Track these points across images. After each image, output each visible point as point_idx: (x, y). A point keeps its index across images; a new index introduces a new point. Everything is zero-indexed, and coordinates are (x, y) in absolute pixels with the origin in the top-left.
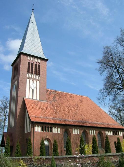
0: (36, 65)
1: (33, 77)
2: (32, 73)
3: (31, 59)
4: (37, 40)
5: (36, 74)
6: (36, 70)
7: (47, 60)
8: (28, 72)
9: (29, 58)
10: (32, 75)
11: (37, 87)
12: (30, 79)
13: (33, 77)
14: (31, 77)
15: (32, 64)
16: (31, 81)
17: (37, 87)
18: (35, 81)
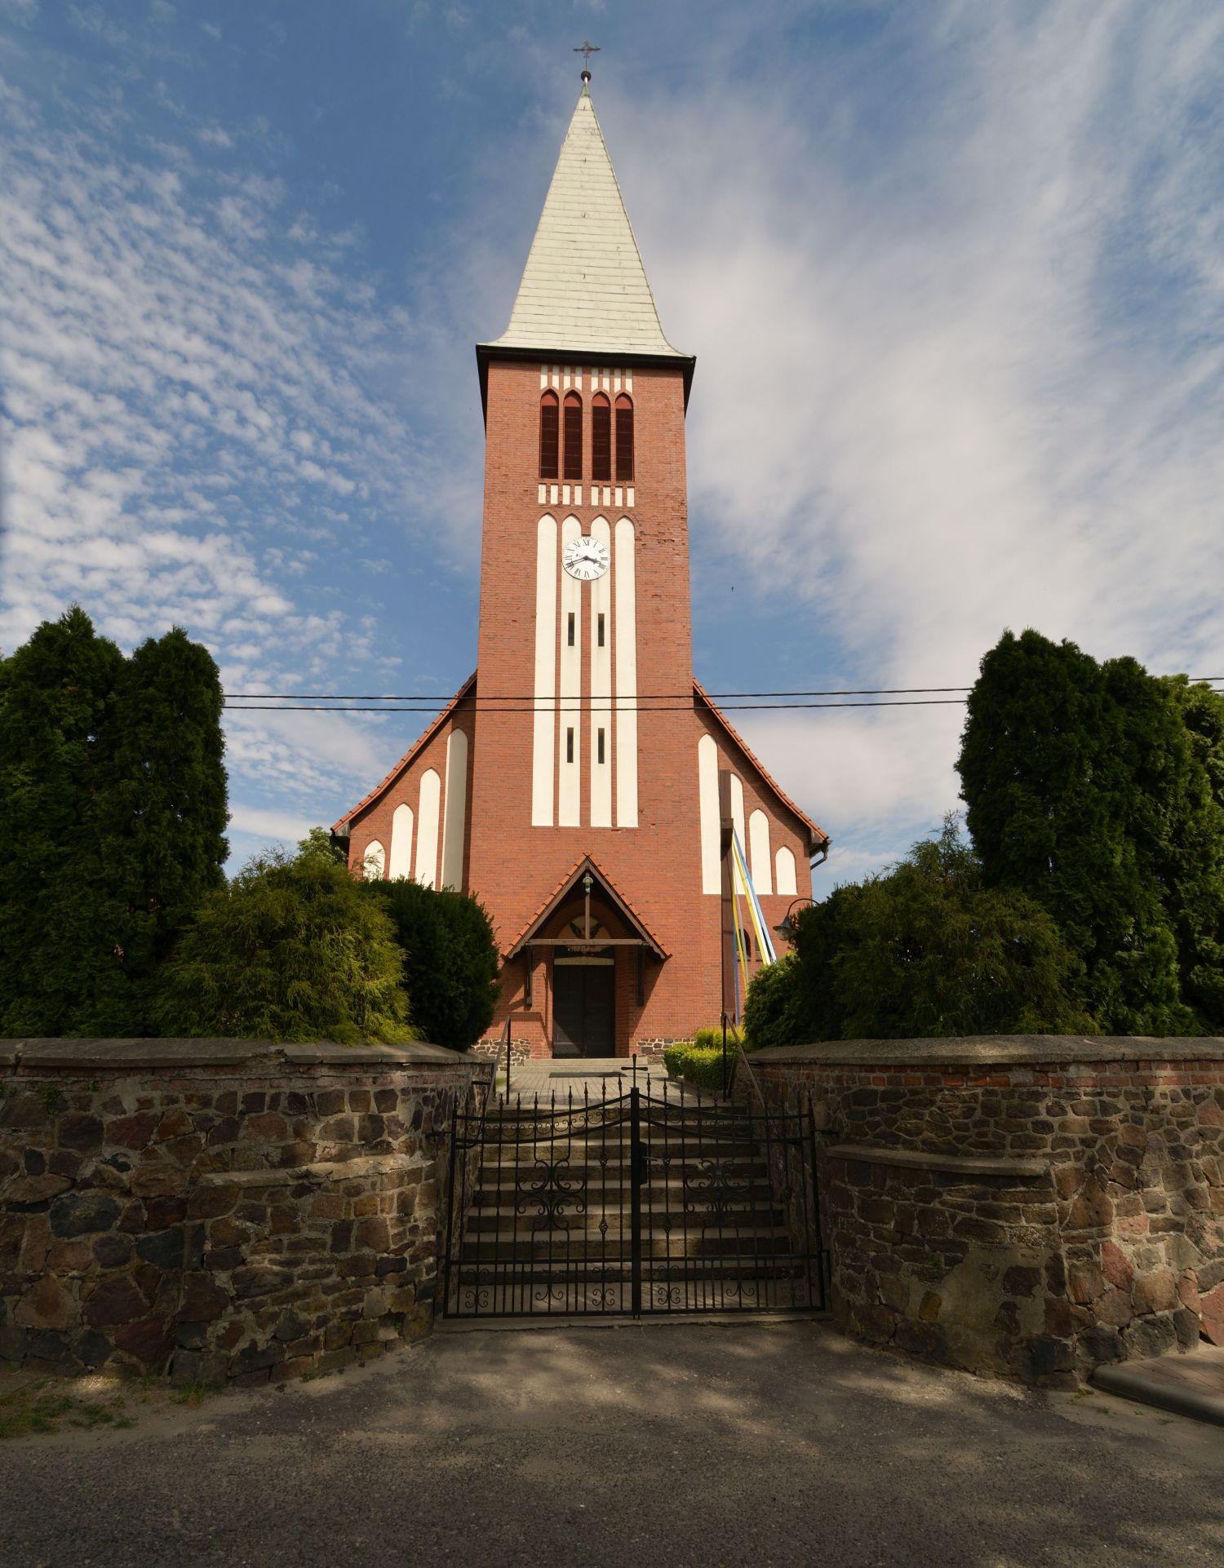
0: (601, 414)
1: (586, 496)
2: (574, 473)
3: (562, 381)
4: (587, 185)
5: (601, 474)
6: (600, 449)
7: (699, 701)
8: (548, 471)
9: (546, 379)
10: (578, 490)
11: (613, 564)
12: (559, 512)
13: (586, 496)
14: (572, 499)
15: (574, 415)
16: (571, 526)
17: (613, 564)
18: (600, 526)
